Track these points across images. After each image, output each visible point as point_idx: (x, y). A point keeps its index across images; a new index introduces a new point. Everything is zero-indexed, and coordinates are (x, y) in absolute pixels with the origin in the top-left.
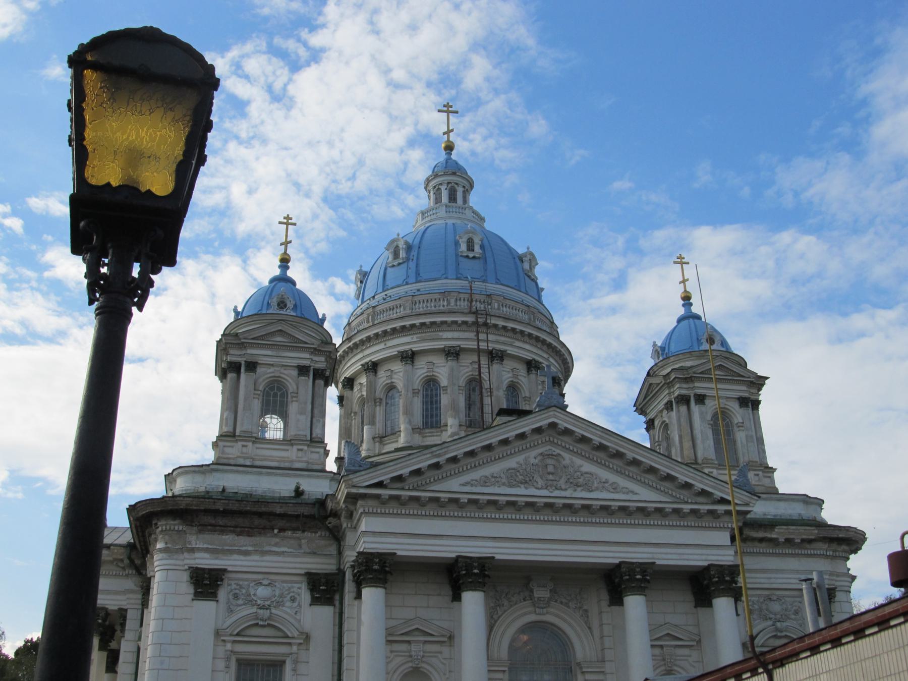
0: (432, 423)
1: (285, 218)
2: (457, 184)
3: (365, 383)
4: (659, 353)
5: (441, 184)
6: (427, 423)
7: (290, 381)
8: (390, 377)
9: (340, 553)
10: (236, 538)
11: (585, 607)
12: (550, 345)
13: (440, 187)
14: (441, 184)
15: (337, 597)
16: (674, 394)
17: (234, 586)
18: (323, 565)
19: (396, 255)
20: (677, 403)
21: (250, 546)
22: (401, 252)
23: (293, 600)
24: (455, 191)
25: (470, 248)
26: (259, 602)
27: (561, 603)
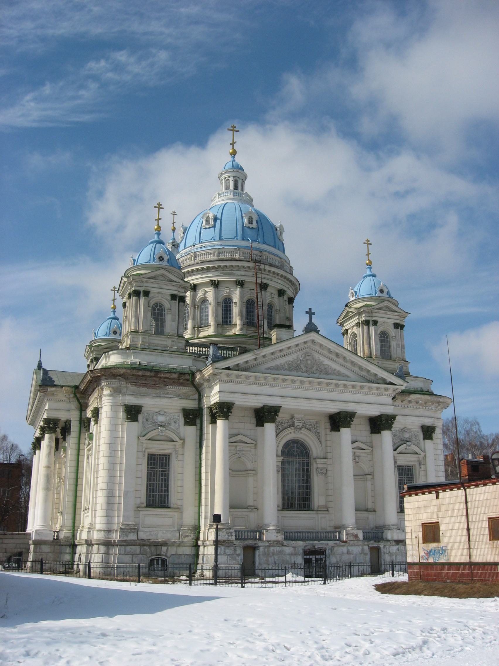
0: (227, 321)
1: (157, 204)
2: (239, 177)
3: (189, 295)
4: (353, 294)
5: (229, 177)
6: (225, 321)
7: (167, 303)
8: (205, 294)
9: (200, 400)
10: (147, 390)
11: (318, 431)
12: (288, 279)
13: (230, 179)
14: (229, 177)
15: (198, 421)
16: (361, 319)
17: (146, 414)
18: (191, 404)
19: (207, 222)
20: (362, 324)
21: (154, 394)
22: (211, 220)
23: (175, 422)
24: (238, 182)
25: (250, 222)
26: (159, 423)
27: (307, 429)
